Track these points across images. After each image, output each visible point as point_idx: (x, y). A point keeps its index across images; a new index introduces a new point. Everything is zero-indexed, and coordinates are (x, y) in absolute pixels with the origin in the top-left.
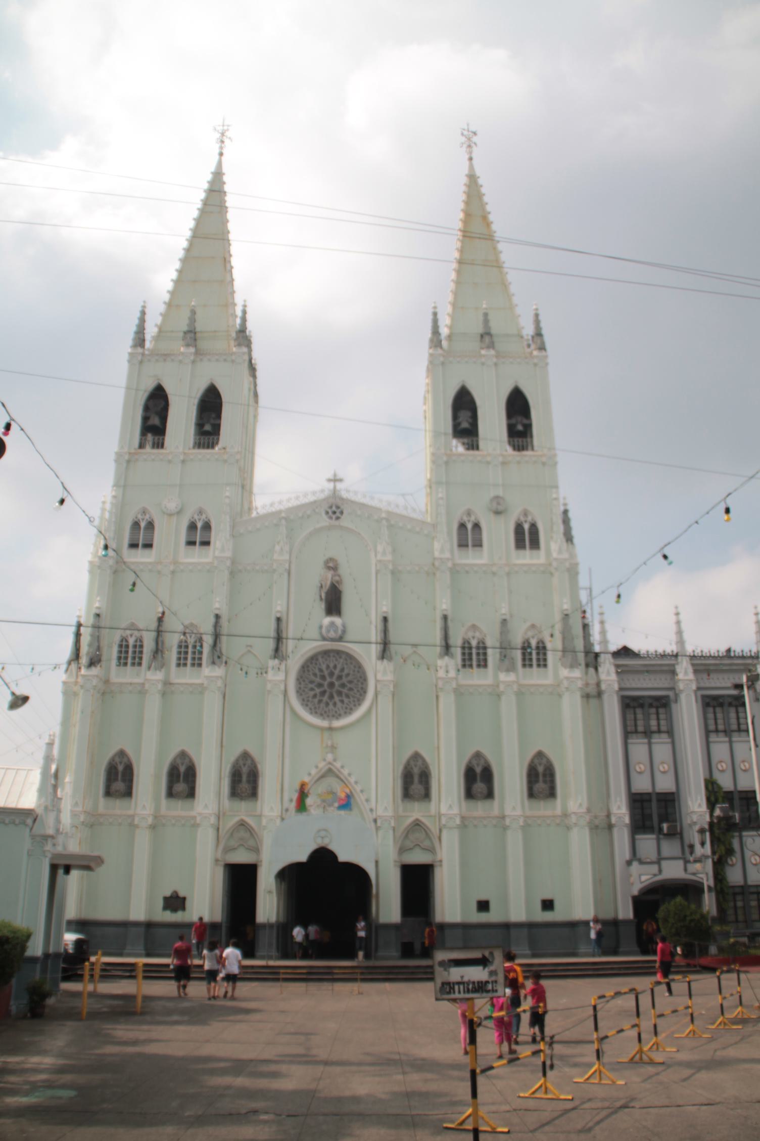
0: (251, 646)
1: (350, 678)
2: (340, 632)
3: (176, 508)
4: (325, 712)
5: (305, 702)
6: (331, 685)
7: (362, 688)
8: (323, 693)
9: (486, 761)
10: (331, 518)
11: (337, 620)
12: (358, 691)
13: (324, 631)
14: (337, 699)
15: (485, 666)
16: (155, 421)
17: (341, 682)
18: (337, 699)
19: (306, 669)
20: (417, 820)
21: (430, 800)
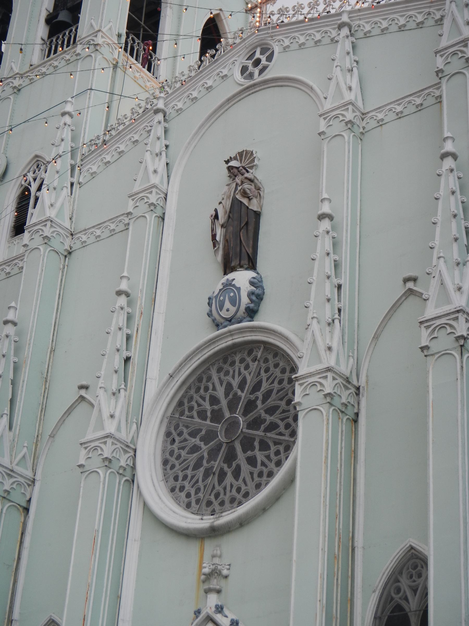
1: (270, 402)
2: (245, 300)
4: (217, 496)
8: (213, 454)
17: (252, 416)
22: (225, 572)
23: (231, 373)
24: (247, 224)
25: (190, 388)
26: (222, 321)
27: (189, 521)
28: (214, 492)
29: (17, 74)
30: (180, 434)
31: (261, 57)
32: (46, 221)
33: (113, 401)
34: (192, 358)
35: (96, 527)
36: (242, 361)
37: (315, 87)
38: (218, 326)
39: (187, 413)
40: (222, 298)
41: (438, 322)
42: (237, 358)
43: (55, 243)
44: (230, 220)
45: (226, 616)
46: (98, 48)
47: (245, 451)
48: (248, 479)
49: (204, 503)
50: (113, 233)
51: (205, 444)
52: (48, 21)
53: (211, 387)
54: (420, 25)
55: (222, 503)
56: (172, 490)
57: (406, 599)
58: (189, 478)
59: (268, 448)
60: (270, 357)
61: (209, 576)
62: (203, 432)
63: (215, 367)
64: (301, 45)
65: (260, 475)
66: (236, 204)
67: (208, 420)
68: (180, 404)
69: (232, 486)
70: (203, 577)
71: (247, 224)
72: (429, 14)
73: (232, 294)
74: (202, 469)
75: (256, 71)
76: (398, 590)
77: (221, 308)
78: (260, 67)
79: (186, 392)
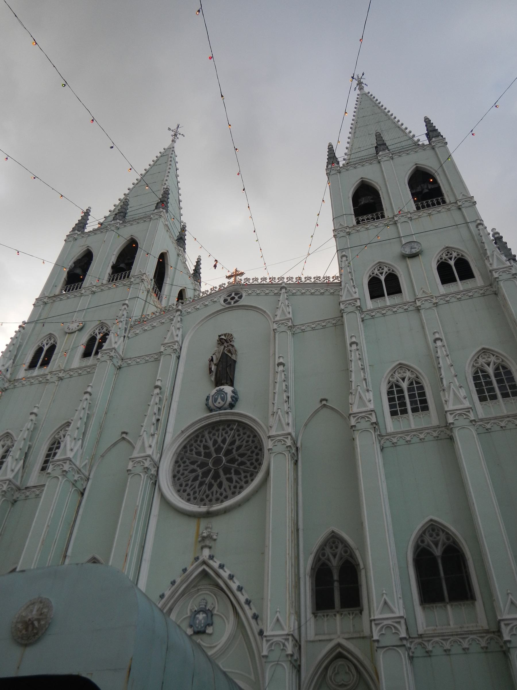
0: (126, 433)
1: (241, 451)
2: (229, 399)
3: (78, 326)
4: (207, 496)
5: (180, 490)
6: (217, 462)
7: (257, 460)
8: (205, 474)
9: (449, 536)
10: (230, 303)
11: (228, 389)
12: (252, 464)
13: (210, 401)
14: (223, 477)
15: (426, 408)
16: (78, 271)
17: (230, 457)
18: (223, 477)
19: (188, 448)
20: (339, 645)
21: (361, 612)
22: (215, 537)
23: (217, 434)
24: (230, 365)
25: (191, 440)
26: (215, 408)
27: (191, 507)
28: (206, 494)
29: (95, 285)
30: (184, 462)
31: (235, 296)
32: (112, 349)
33: (151, 439)
34: (196, 424)
35: (137, 504)
36: (223, 429)
37: (267, 312)
38: (211, 410)
39: (188, 451)
40: (216, 397)
41: (361, 415)
42: (221, 428)
43: (115, 361)
44: (220, 362)
45: (215, 562)
46: (143, 281)
47: (225, 474)
48: (228, 489)
49: (199, 500)
50: (147, 362)
51: (200, 469)
52: (113, 267)
53: (204, 440)
54: (322, 294)
55: (211, 501)
56: (179, 491)
57: (329, 560)
58: (189, 485)
59: (240, 474)
60: (241, 429)
61: (204, 538)
62: (199, 463)
63: (207, 431)
64: (258, 294)
65: (235, 487)
66: (224, 355)
67: (202, 456)
68: (185, 447)
69: (217, 492)
70: (200, 539)
71: (230, 365)
72: (327, 290)
73: (222, 396)
74: (198, 482)
75: (232, 302)
76: (324, 555)
77: (215, 402)
78: (235, 300)
79: (189, 441)
